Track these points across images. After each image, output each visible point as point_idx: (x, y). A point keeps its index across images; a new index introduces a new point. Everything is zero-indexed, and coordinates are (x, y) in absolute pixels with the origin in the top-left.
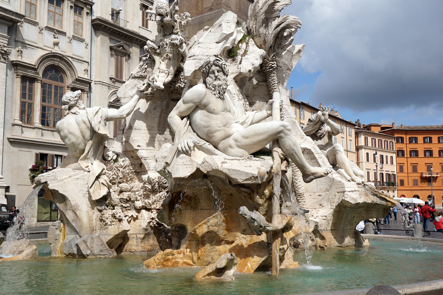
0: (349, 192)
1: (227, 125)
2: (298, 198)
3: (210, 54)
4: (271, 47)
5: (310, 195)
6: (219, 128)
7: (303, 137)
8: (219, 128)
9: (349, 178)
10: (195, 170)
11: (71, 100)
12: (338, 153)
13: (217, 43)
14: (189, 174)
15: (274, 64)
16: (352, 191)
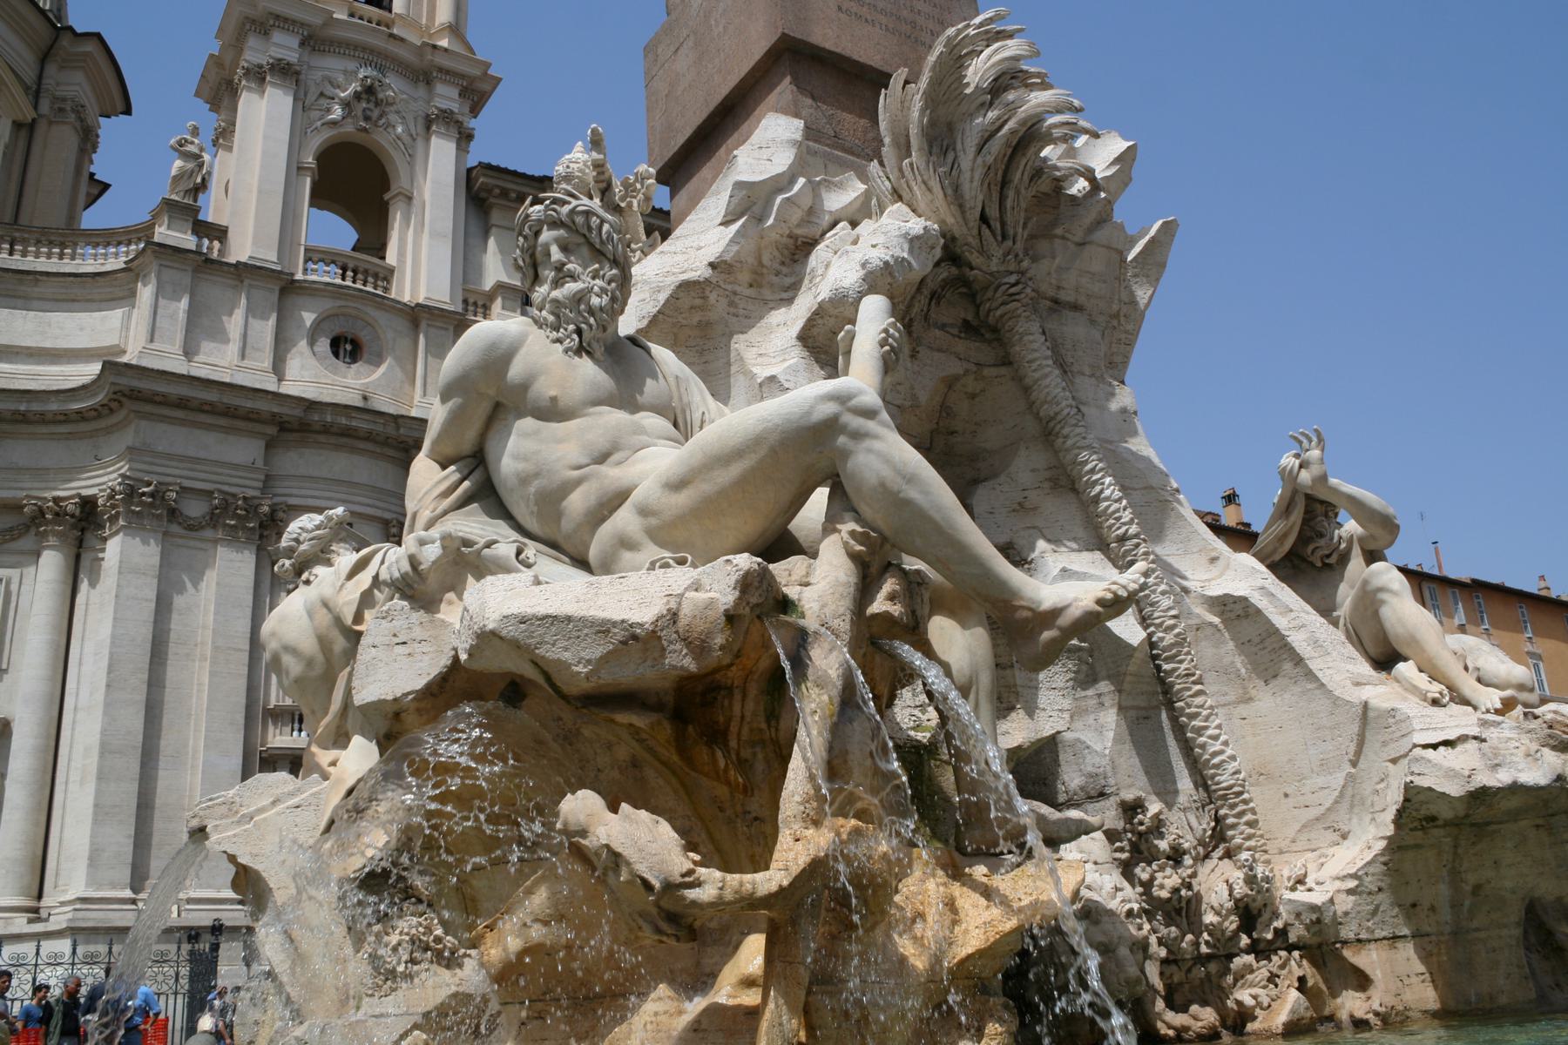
0: (1435, 747)
1: (615, 457)
2: (1222, 812)
3: (698, 264)
4: (984, 218)
5: (1286, 795)
6: (576, 473)
7: (1214, 554)
8: (576, 473)
9: (1435, 689)
10: (445, 661)
11: (301, 539)
12: (1382, 602)
13: (725, 223)
14: (419, 684)
15: (1017, 284)
16: (1447, 743)
